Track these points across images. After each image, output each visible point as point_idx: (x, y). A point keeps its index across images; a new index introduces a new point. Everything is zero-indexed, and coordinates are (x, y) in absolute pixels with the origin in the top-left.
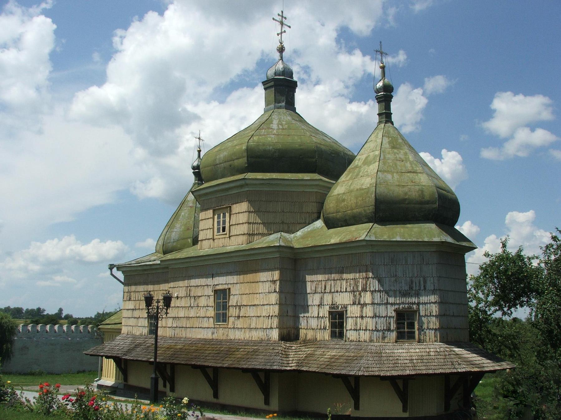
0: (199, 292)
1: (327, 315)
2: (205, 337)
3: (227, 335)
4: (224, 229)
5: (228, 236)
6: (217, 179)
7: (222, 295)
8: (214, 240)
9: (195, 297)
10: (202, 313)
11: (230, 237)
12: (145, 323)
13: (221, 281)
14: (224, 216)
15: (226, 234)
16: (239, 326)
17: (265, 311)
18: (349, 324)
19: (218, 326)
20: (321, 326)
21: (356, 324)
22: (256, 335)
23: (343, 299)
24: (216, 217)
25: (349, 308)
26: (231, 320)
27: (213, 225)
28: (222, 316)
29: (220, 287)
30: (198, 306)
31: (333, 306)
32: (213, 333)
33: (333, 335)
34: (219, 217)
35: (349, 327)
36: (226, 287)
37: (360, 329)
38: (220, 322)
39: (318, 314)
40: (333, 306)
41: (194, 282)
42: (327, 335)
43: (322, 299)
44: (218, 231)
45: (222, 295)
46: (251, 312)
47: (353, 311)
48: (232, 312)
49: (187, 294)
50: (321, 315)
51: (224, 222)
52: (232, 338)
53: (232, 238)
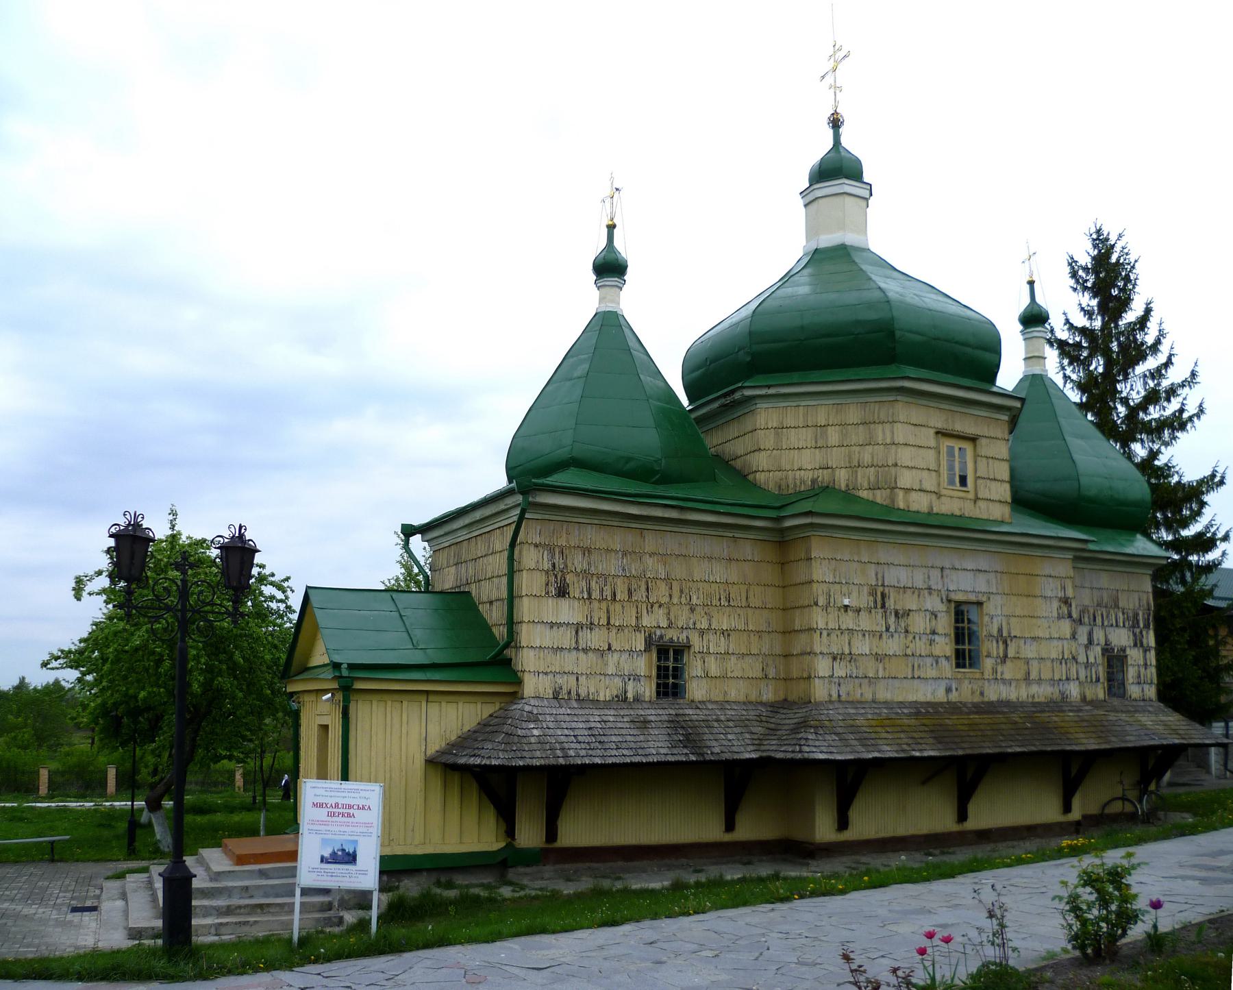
0: (910, 602)
1: (1100, 660)
2: (929, 698)
3: (982, 694)
4: (963, 481)
5: (971, 496)
6: (946, 372)
10: (921, 646)
12: (644, 665)
16: (1007, 676)
17: (1053, 650)
18: (1131, 673)
21: (1139, 676)
22: (1042, 692)
24: (944, 450)
25: (1128, 651)
26: (988, 664)
28: (964, 658)
29: (960, 597)
30: (907, 631)
32: (949, 690)
33: (1110, 691)
35: (1131, 680)
38: (964, 667)
43: (1090, 634)
44: (951, 482)
46: (1030, 651)
47: (1134, 655)
48: (990, 648)
49: (875, 602)
50: (1092, 660)
52: (994, 698)
53: (980, 503)
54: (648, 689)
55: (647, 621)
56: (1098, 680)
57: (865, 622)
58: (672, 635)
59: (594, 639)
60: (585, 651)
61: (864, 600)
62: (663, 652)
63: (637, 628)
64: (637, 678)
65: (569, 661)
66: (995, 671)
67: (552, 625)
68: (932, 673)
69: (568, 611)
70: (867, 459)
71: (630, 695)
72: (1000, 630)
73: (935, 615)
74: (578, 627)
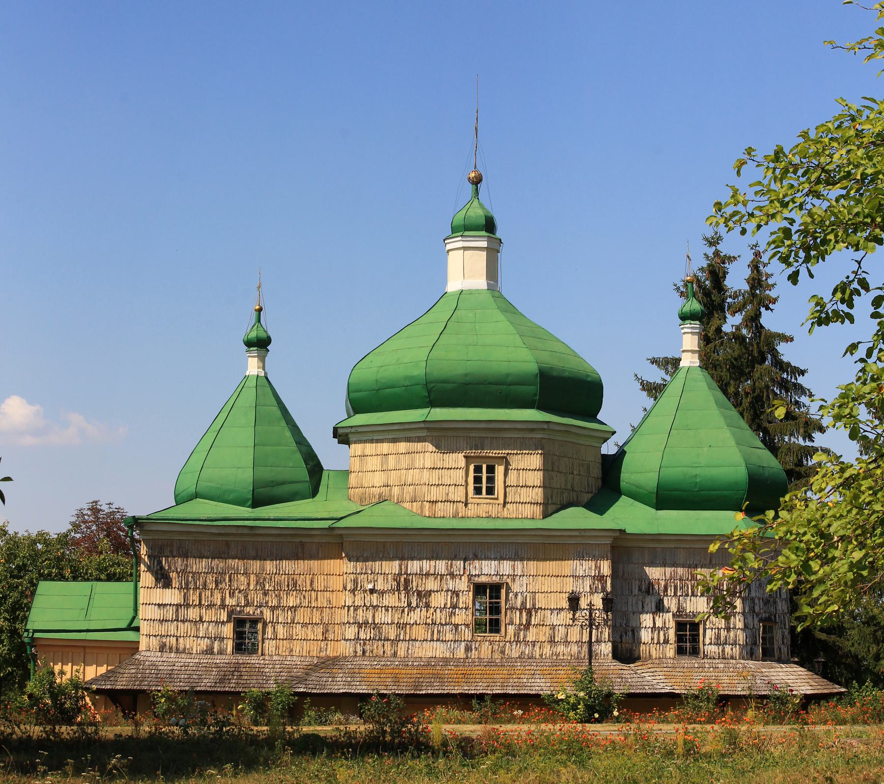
0: (431, 584)
4: (490, 491)
5: (501, 501)
7: (489, 593)
8: (466, 505)
9: (419, 594)
10: (440, 617)
11: (505, 503)
12: (228, 630)
13: (487, 570)
14: (491, 469)
15: (497, 499)
19: (479, 639)
20: (659, 639)
23: (699, 605)
24: (472, 467)
27: (466, 481)
29: (483, 579)
31: (680, 612)
32: (468, 649)
33: (680, 651)
34: (478, 469)
35: (707, 641)
36: (496, 579)
37: (726, 644)
38: (485, 632)
39: (654, 623)
40: (680, 612)
41: (414, 566)
42: (670, 651)
44: (478, 491)
45: (489, 593)
51: (491, 480)
53: (508, 506)
54: (229, 645)
55: (229, 601)
56: (666, 641)
57: (390, 600)
58: (250, 610)
59: (193, 613)
60: (183, 621)
61: (391, 584)
62: (239, 623)
63: (223, 606)
64: (222, 639)
65: (172, 628)
66: (516, 634)
67: (159, 605)
68: (449, 636)
69: (172, 596)
70: (410, 481)
71: (215, 650)
72: (524, 603)
73: (456, 593)
74: (178, 606)
